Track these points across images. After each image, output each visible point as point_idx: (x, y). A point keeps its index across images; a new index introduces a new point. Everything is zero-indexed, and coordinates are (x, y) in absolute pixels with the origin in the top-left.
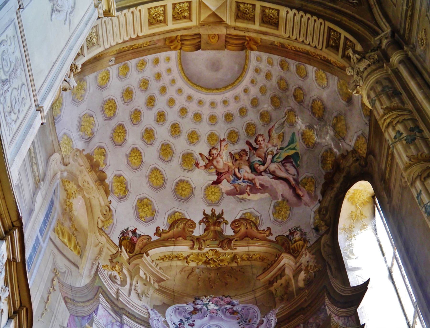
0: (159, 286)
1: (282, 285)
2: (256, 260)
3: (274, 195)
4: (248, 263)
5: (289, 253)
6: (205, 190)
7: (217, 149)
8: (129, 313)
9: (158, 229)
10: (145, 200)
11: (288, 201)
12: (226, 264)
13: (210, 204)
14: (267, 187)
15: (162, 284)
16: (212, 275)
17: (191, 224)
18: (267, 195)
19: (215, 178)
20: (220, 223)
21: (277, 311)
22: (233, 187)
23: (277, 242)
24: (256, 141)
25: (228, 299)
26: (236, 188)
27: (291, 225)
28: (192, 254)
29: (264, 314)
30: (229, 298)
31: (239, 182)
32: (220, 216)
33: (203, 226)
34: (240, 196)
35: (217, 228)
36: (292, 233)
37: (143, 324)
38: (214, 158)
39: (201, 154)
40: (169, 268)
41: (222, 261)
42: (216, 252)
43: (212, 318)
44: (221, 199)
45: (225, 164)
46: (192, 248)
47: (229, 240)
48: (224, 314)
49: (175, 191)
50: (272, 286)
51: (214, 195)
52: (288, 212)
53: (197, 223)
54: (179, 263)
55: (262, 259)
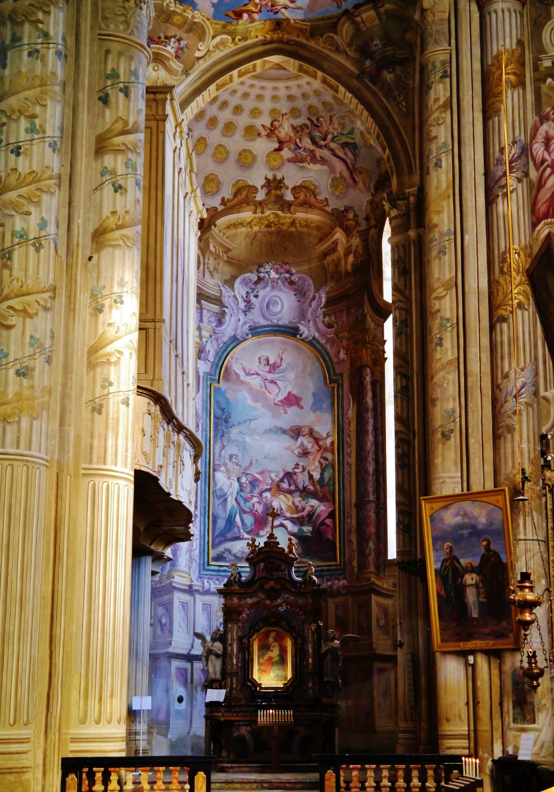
0: (228, 257)
1: (333, 261)
2: (313, 228)
3: (332, 170)
4: (304, 230)
5: (342, 228)
6: (267, 157)
7: (279, 121)
8: (206, 296)
9: (223, 199)
10: (210, 177)
11: (345, 179)
12: (286, 228)
13: (272, 169)
14: (327, 161)
15: (230, 254)
16: (273, 239)
17: (254, 189)
18: (325, 168)
19: (276, 145)
20: (281, 187)
21: (327, 289)
22: (293, 155)
23: (332, 214)
24: (318, 119)
25: (287, 267)
26: (296, 156)
27: (347, 202)
28: (255, 218)
29: (317, 290)
30: (287, 265)
31: (300, 151)
32: (281, 181)
33: (265, 190)
34: (301, 165)
35: (279, 192)
36: (347, 209)
37: (217, 303)
38: (275, 129)
39: (263, 126)
40: (235, 236)
41: (282, 224)
42: (277, 215)
43: (273, 288)
44: (283, 164)
45: (286, 134)
46: (255, 212)
47: (289, 205)
48: (284, 284)
49: (238, 160)
50: (326, 259)
51: (276, 161)
52: (344, 190)
53: (259, 187)
54: (243, 230)
55: (318, 228)
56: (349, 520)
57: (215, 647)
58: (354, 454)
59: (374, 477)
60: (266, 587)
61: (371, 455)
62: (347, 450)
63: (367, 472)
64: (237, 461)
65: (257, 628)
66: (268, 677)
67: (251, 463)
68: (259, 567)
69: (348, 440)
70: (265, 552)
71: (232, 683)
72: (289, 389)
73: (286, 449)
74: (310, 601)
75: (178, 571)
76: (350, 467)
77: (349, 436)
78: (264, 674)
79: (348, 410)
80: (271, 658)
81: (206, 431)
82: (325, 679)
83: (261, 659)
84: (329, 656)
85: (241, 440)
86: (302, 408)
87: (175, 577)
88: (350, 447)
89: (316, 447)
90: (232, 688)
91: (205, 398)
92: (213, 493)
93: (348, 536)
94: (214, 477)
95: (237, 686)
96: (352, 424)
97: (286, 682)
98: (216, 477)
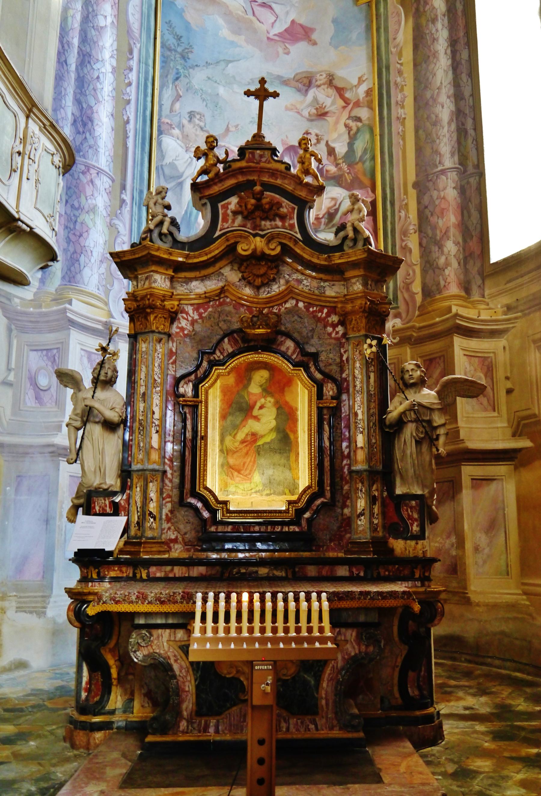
56: (403, 214)
57: (102, 402)
58: (410, 102)
59: (453, 126)
60: (243, 249)
61: (444, 91)
62: (396, 96)
63: (436, 123)
64: (202, 124)
65: (218, 355)
66: (247, 485)
67: (227, 130)
68: (226, 207)
69: (399, 80)
70: (241, 171)
71: (146, 499)
72: (292, 16)
73: (287, 109)
74: (358, 287)
75: (82, 292)
76: (403, 124)
77: (400, 72)
78: (238, 478)
79: (397, 31)
80: (254, 437)
81: (147, 64)
82: (399, 491)
83: (228, 439)
84: (410, 430)
85: (210, 91)
86: (315, 44)
87: (74, 302)
88: (402, 90)
89: (341, 103)
90: (144, 513)
91: (145, 10)
92: (157, 168)
93: (403, 241)
94: (159, 144)
95: (160, 508)
96: (404, 53)
97: (295, 498)
98: (164, 145)
